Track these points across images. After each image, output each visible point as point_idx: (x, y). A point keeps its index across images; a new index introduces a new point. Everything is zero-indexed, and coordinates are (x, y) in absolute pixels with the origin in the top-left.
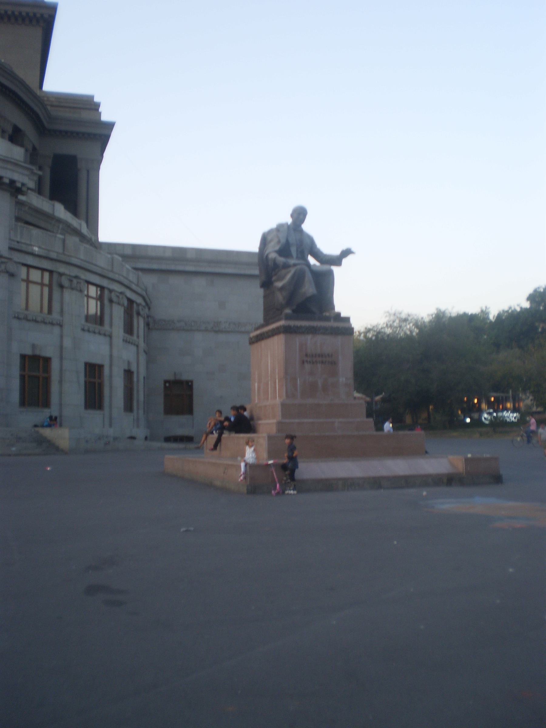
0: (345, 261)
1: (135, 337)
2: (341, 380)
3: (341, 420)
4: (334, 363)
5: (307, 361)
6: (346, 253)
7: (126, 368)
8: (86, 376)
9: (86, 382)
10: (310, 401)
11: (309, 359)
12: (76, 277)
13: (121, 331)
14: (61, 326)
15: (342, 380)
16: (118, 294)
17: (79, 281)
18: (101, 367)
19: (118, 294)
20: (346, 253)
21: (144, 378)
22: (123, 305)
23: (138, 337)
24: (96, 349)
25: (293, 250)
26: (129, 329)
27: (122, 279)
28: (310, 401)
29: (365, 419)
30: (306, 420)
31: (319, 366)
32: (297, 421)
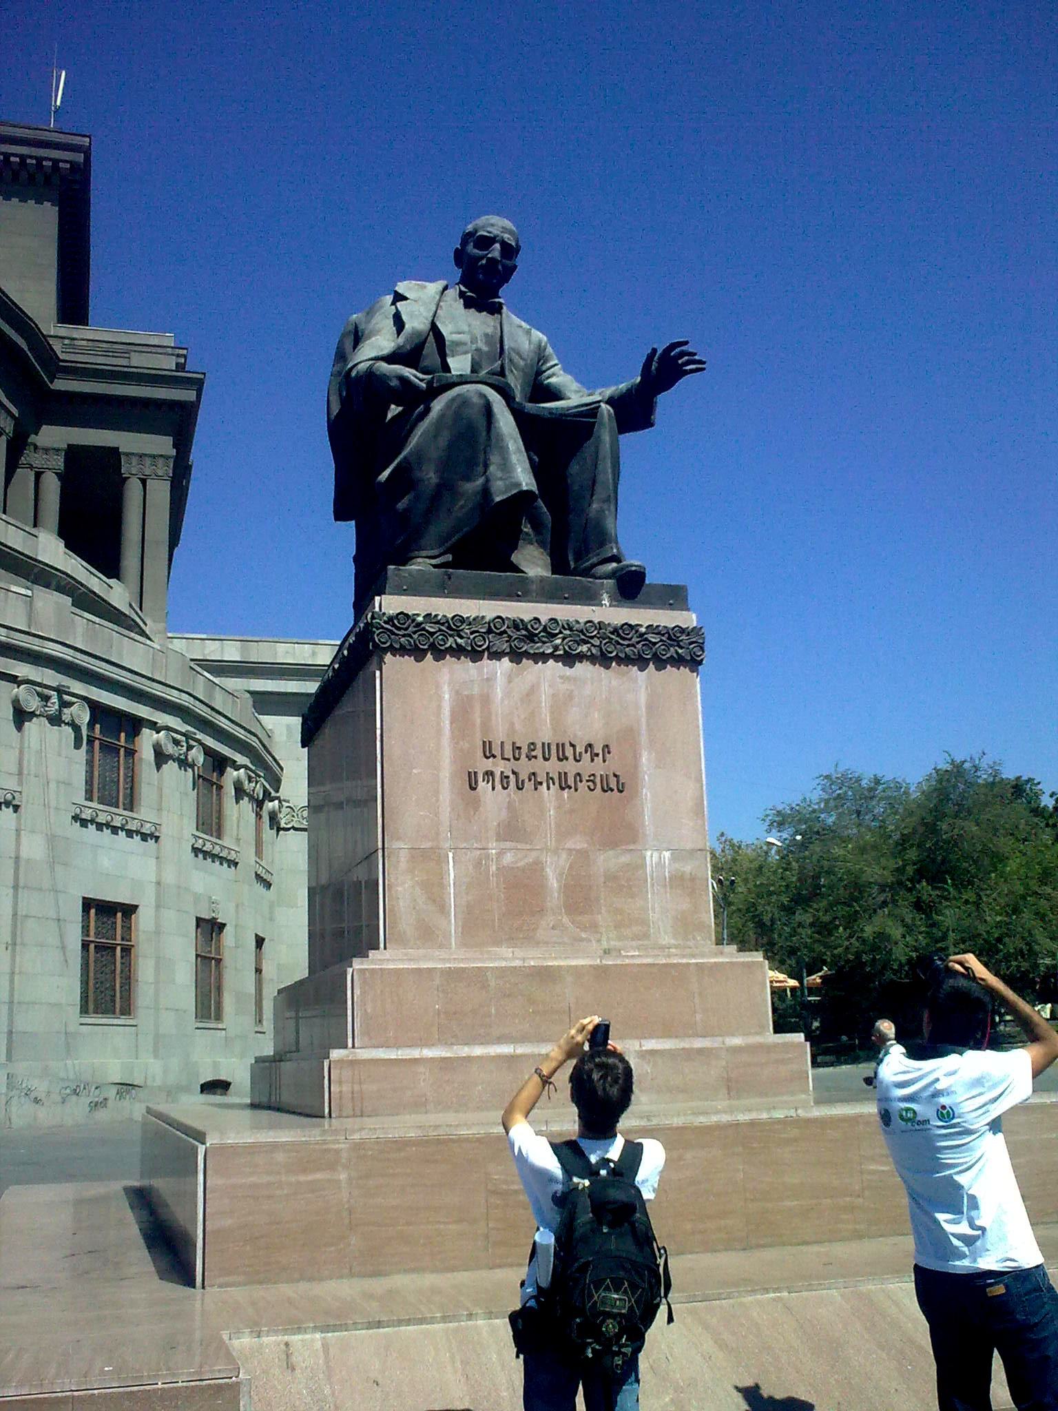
0: (664, 401)
1: (227, 841)
2: (651, 857)
3: (650, 1044)
4: (616, 785)
5: (489, 774)
6: (666, 369)
7: (206, 915)
8: (86, 929)
9: (85, 946)
10: (507, 957)
11: (499, 767)
12: (60, 691)
13: (189, 826)
14: (16, 808)
15: (656, 858)
16: (179, 737)
17: (66, 697)
18: (129, 910)
19: (179, 737)
20: (666, 369)
21: (260, 942)
22: (192, 766)
23: (238, 840)
24: (117, 868)
25: (459, 365)
26: (211, 822)
27: (185, 700)
28: (507, 957)
29: (771, 1037)
30: (478, 1051)
31: (549, 795)
32: (428, 1053)
